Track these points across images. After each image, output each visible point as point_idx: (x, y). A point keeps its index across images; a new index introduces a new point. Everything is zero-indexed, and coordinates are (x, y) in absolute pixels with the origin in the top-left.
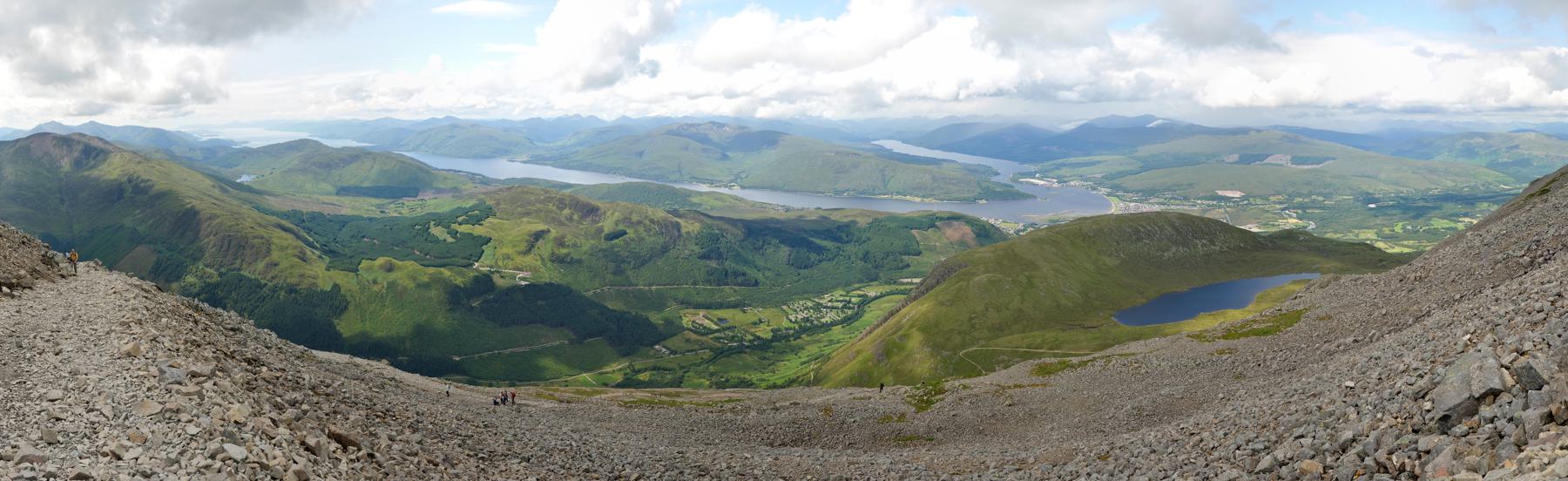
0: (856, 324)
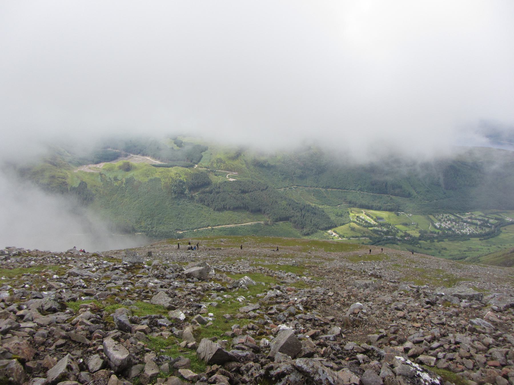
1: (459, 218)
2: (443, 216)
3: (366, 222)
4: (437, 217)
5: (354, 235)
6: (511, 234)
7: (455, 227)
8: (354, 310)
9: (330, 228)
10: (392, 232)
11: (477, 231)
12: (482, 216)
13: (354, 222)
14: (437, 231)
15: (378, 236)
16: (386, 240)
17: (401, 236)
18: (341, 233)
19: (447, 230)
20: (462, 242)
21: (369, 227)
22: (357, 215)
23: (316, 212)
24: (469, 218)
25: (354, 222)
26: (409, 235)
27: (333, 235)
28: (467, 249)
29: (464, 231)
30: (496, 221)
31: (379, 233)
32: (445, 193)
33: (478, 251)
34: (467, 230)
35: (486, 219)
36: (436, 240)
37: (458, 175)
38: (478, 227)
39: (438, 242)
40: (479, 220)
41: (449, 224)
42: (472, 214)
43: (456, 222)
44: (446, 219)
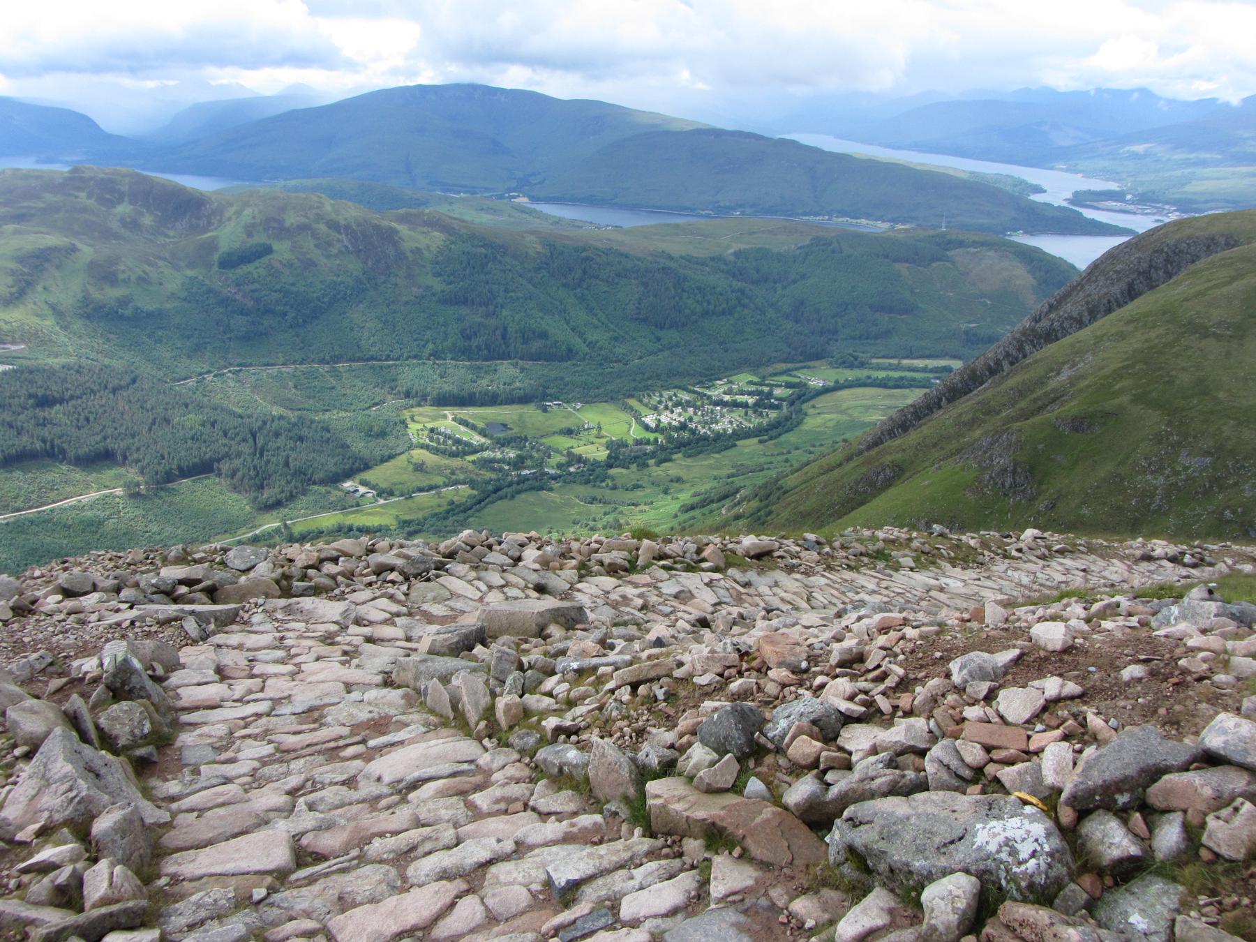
0: (790, 437)
1: (703, 395)
2: (661, 396)
3: (458, 442)
4: (646, 400)
5: (424, 484)
6: (828, 416)
7: (696, 419)
8: (283, 209)
9: (349, 475)
10: (531, 457)
11: (750, 421)
12: (755, 384)
13: (422, 446)
14: (651, 436)
15: (493, 476)
16: (518, 483)
17: (560, 466)
18: (384, 485)
19: (676, 429)
20: (717, 456)
21: (465, 453)
22: (429, 426)
23: (304, 432)
24: (725, 393)
25: (422, 446)
26: (579, 459)
27: (358, 495)
28: (733, 471)
29: (717, 427)
30: (790, 391)
31: (496, 465)
32: (659, 339)
33: (762, 470)
34: (726, 423)
35: (766, 389)
36: (651, 462)
37: (683, 290)
38: (750, 412)
39: (658, 464)
40: (750, 394)
41: (680, 415)
42: (732, 382)
43: (696, 408)
44: (670, 404)
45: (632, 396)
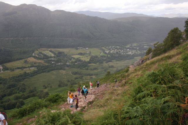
39: (107, 62)
45: (103, 47)
